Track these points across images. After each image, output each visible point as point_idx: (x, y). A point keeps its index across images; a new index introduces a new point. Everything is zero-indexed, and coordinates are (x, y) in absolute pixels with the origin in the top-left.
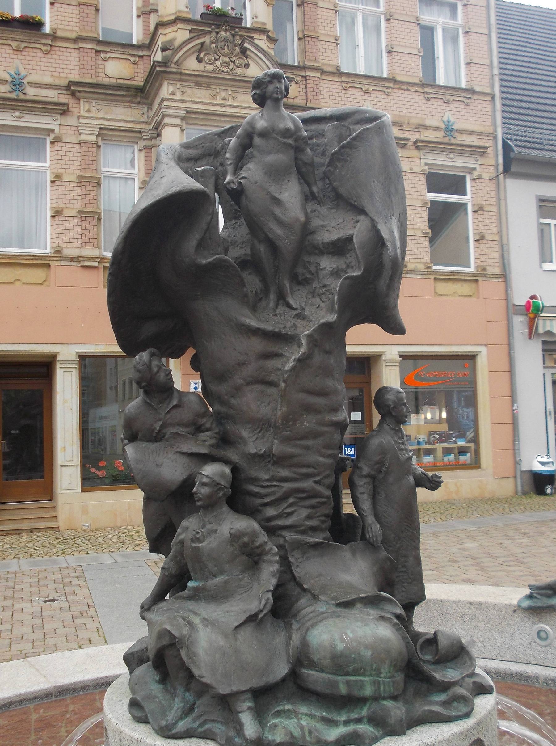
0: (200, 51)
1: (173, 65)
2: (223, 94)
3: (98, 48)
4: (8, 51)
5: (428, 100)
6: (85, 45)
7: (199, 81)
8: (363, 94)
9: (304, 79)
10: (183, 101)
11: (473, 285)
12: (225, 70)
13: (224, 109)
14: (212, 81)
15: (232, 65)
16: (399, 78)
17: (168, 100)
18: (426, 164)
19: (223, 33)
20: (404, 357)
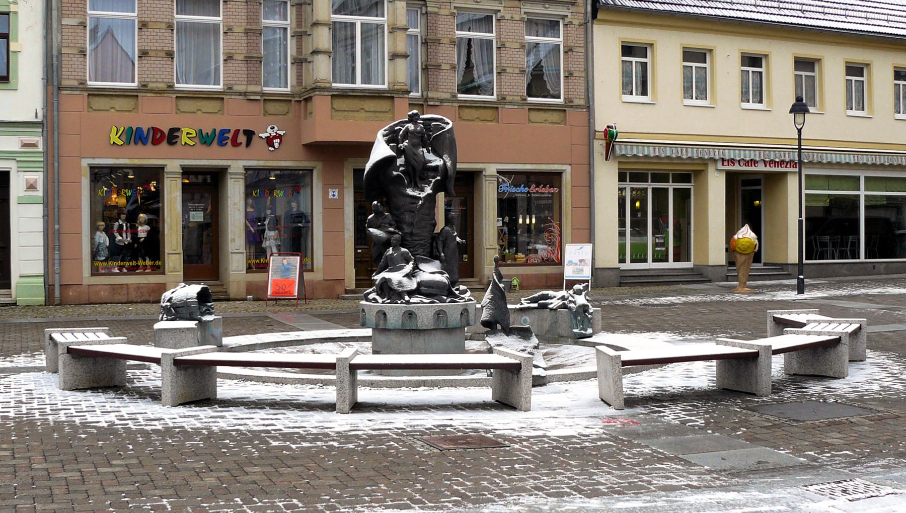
11: (562, 114)
18: (525, 13)
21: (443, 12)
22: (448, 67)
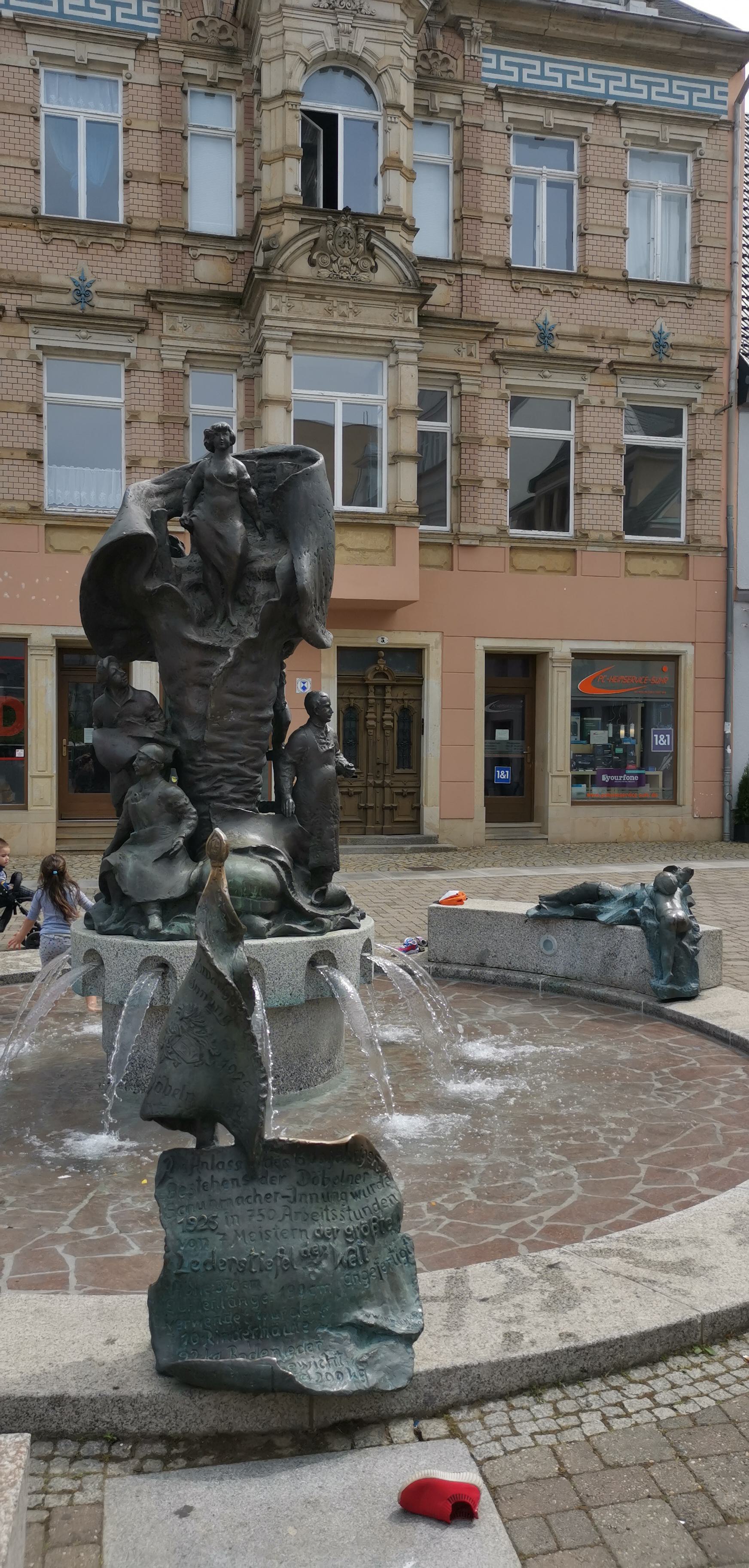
0: (312, 250)
1: (276, 272)
2: (344, 309)
3: (186, 242)
4: (70, 249)
5: (632, 302)
6: (168, 239)
7: (310, 290)
8: (540, 297)
9: (459, 278)
10: (288, 320)
11: (681, 562)
12: (345, 275)
13: (342, 329)
14: (328, 291)
15: (354, 269)
16: (591, 273)
17: (270, 318)
18: (624, 395)
19: (342, 225)
20: (576, 655)
21: (486, 393)
22: (493, 484)
